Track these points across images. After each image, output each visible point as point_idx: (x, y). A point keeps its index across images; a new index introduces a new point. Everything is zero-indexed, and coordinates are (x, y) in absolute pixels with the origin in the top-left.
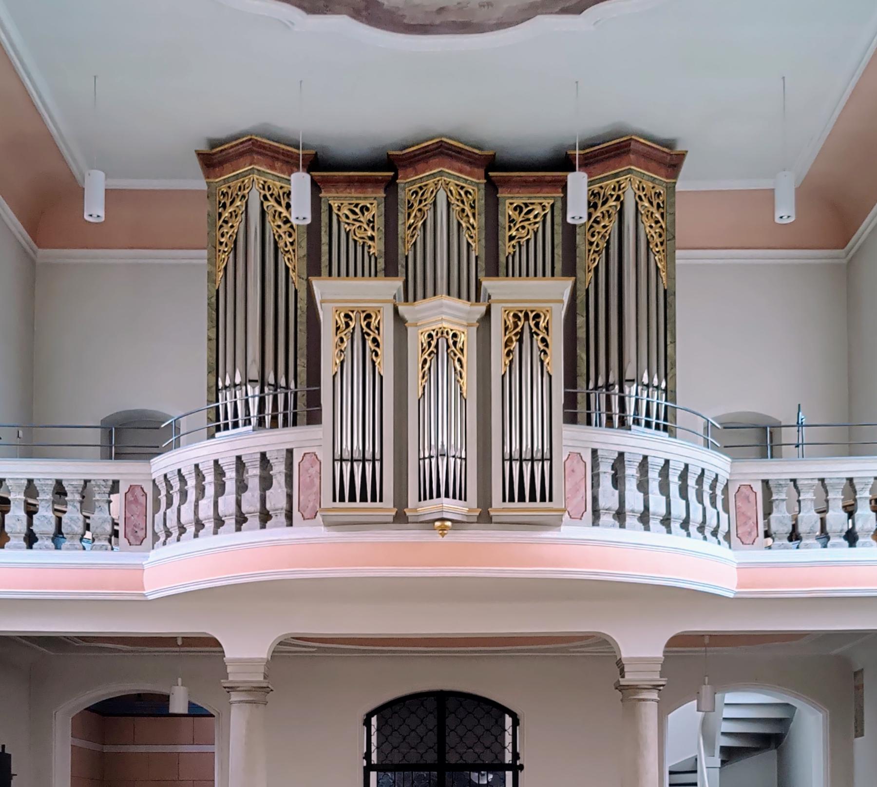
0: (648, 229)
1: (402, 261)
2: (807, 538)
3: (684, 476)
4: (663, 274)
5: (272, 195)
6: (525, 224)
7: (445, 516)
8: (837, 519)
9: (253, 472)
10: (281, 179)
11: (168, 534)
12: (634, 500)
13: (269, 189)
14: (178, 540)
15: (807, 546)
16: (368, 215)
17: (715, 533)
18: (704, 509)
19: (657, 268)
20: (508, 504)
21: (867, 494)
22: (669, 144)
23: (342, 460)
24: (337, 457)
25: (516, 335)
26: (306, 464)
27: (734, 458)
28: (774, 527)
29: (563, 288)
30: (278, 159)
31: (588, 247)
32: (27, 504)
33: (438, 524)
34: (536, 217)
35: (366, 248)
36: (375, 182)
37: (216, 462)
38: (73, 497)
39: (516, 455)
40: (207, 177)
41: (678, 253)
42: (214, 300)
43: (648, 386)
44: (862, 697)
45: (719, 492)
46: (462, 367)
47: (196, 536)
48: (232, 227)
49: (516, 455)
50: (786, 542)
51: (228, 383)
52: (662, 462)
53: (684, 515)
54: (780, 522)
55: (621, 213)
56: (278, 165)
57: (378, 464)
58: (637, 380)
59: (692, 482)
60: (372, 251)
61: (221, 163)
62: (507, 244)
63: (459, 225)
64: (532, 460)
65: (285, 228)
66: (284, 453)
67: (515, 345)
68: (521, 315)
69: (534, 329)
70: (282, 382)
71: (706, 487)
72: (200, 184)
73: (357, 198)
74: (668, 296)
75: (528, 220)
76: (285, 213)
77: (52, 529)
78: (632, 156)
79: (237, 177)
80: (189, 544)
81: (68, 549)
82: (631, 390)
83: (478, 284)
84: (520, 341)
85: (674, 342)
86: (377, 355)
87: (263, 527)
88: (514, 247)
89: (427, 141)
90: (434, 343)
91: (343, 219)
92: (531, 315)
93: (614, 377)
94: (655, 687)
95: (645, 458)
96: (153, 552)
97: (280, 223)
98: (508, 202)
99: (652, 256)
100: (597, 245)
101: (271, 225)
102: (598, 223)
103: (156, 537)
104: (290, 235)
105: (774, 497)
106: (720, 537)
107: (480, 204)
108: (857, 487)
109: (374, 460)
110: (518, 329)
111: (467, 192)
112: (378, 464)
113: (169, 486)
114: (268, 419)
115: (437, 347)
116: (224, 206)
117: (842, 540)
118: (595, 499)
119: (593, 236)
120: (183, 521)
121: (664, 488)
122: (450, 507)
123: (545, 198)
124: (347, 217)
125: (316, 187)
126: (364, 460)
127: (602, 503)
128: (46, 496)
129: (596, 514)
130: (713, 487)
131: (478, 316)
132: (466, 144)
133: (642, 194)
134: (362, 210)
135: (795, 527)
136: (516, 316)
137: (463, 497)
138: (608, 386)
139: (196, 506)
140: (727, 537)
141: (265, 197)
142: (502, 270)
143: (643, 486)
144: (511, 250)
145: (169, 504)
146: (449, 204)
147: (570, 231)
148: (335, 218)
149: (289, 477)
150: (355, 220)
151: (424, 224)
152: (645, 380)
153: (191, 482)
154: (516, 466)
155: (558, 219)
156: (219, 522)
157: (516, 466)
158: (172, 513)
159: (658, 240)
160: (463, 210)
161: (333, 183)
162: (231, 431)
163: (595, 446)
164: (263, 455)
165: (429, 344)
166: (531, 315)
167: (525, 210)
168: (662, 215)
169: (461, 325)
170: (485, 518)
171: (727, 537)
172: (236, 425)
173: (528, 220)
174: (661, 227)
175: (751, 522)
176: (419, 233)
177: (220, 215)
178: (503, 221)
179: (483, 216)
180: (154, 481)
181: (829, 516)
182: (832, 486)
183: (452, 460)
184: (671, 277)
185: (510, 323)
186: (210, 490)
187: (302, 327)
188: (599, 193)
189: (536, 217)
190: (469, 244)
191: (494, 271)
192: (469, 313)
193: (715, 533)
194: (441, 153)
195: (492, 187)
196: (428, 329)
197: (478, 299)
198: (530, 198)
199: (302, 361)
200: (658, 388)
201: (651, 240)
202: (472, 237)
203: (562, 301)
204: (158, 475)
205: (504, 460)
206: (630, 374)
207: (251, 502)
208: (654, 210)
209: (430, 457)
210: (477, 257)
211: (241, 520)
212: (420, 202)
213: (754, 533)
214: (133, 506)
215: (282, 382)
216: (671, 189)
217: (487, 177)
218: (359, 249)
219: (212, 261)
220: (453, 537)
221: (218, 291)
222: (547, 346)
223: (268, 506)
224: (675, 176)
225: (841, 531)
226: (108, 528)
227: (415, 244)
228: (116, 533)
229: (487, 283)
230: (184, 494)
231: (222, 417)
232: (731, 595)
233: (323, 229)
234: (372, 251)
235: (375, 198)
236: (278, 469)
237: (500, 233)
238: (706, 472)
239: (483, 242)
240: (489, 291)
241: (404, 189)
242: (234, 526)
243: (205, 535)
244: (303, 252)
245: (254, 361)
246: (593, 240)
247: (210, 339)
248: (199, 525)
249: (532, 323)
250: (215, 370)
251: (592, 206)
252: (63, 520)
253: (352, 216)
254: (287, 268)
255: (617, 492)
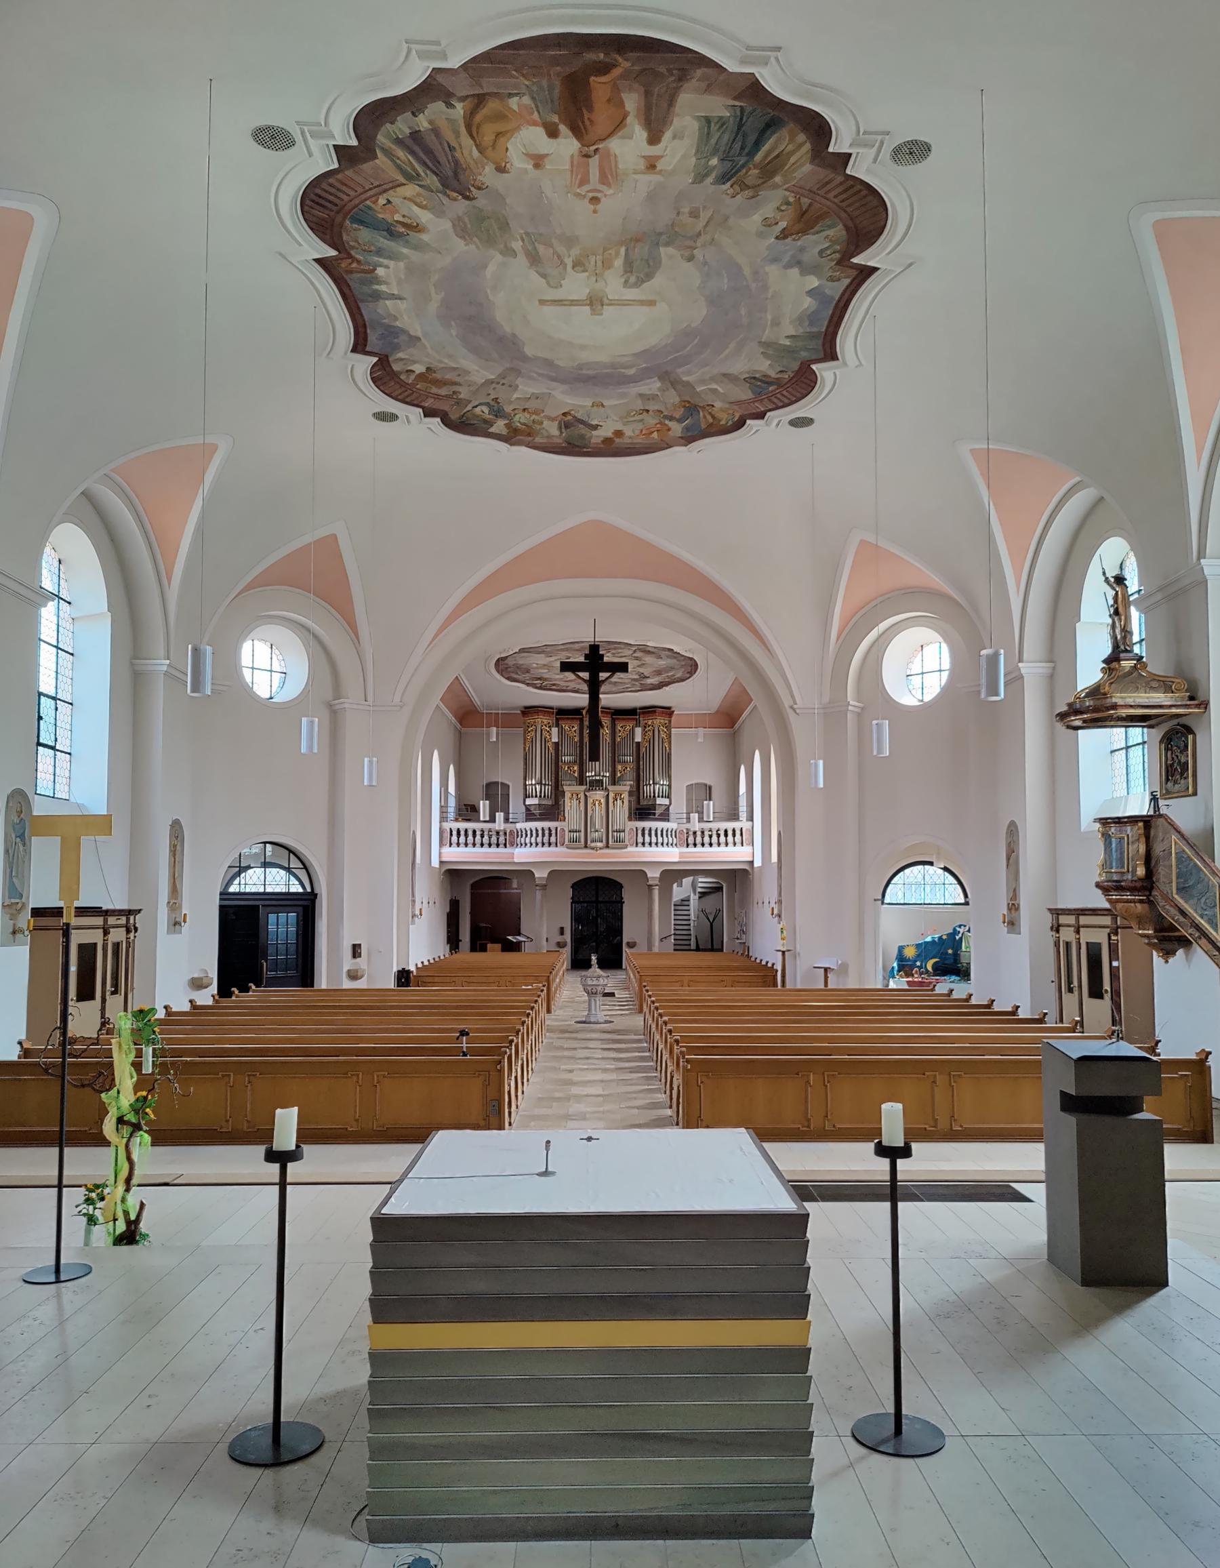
9: (547, 832)
93: (651, 782)
122: (599, 844)
129: (637, 844)
137: (602, 842)
156: (537, 844)
158: (523, 839)
170: (607, 846)
171: (676, 845)
236: (553, 832)
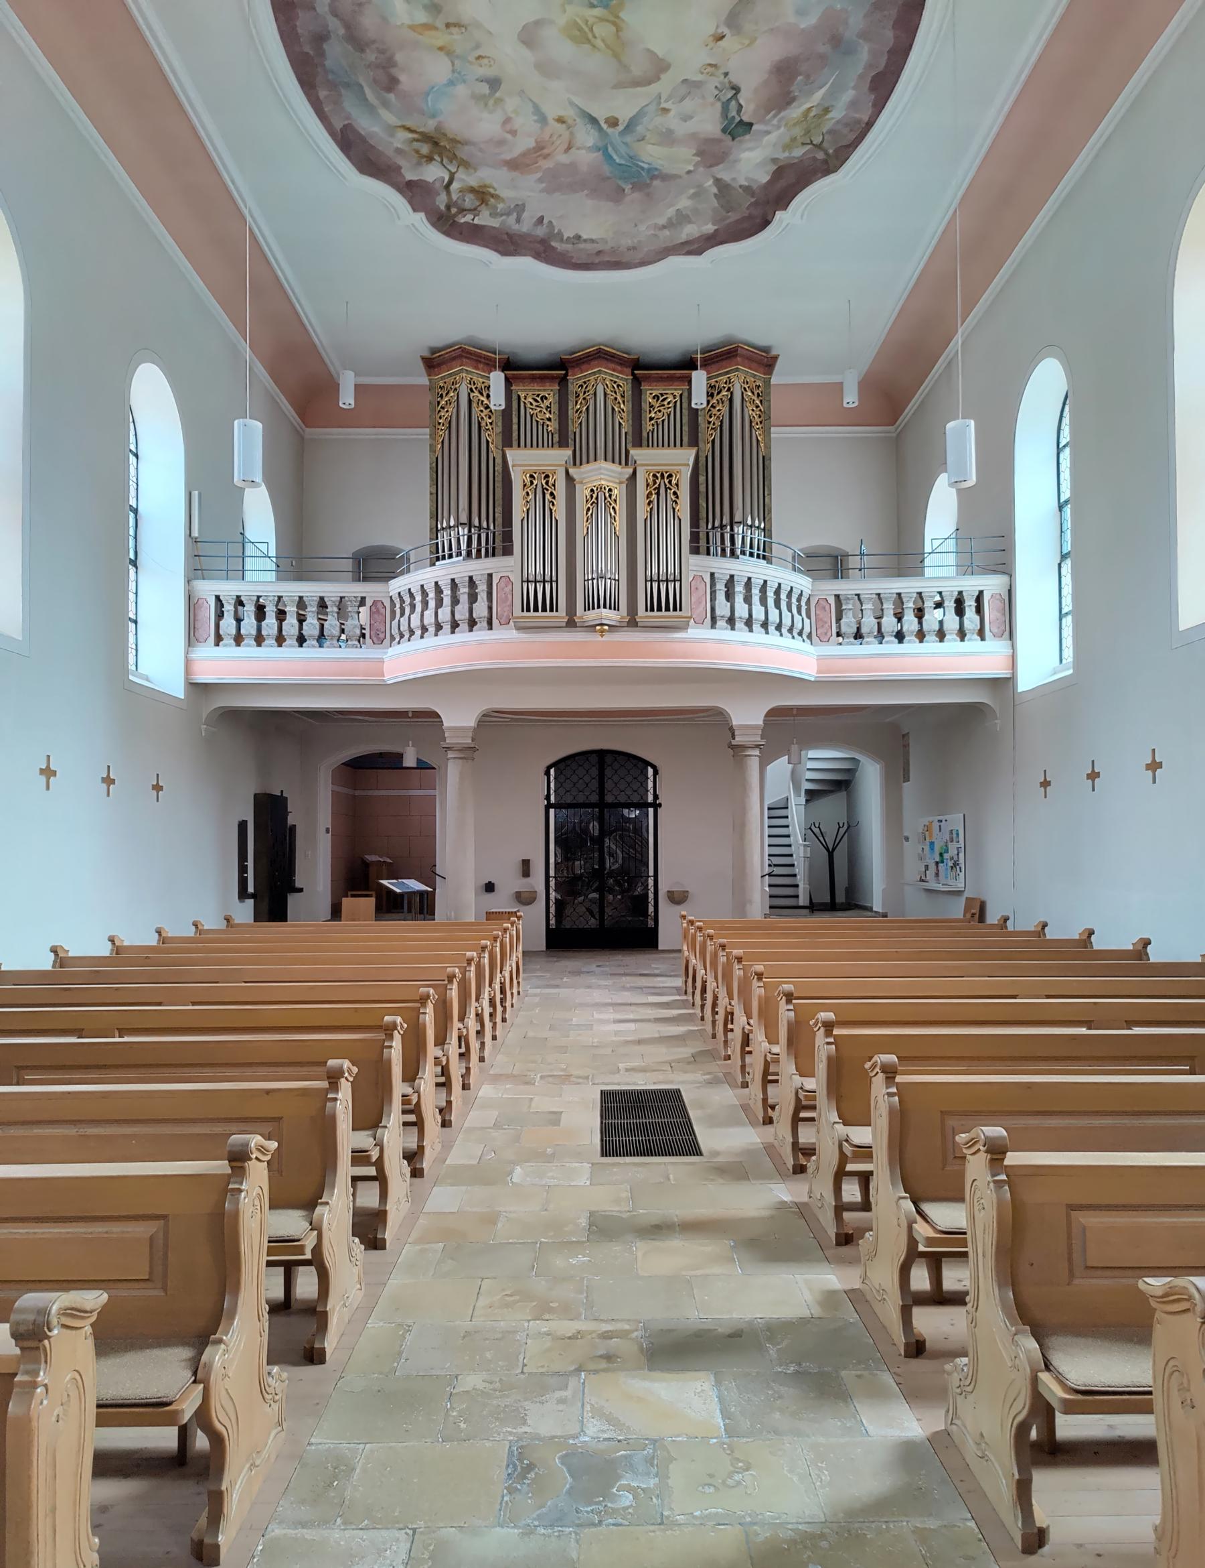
0: (751, 412)
1: (571, 436)
2: (868, 637)
3: (777, 592)
4: (762, 445)
5: (476, 388)
6: (661, 408)
7: (604, 622)
8: (889, 622)
9: (464, 590)
10: (482, 377)
11: (402, 636)
12: (741, 610)
13: (474, 384)
14: (409, 640)
15: (868, 643)
16: (547, 403)
17: (800, 634)
18: (793, 616)
19: (758, 440)
20: (649, 613)
21: (911, 605)
22: (766, 350)
23: (528, 581)
24: (525, 579)
25: (654, 489)
26: (502, 584)
27: (814, 579)
28: (843, 629)
29: (689, 455)
30: (480, 362)
31: (707, 425)
32: (298, 614)
33: (598, 628)
34: (669, 403)
35: (545, 427)
36: (552, 378)
37: (436, 583)
38: (332, 609)
39: (655, 578)
40: (429, 375)
41: (772, 429)
42: (434, 465)
43: (751, 526)
44: (908, 752)
45: (803, 603)
46: (615, 513)
47: (422, 637)
48: (447, 411)
49: (655, 578)
50: (853, 640)
51: (445, 525)
52: (762, 582)
53: (778, 621)
54: (848, 625)
55: (731, 400)
56: (481, 366)
57: (554, 584)
58: (743, 522)
59: (783, 596)
60: (550, 429)
61: (439, 365)
62: (648, 423)
63: (613, 409)
64: (667, 581)
65: (486, 412)
66: (486, 576)
67: (654, 497)
68: (659, 475)
69: (668, 485)
70: (485, 525)
71: (794, 600)
72: (424, 380)
73: (539, 390)
74: (765, 461)
75: (664, 405)
76: (486, 401)
77: (317, 632)
78: (739, 359)
79: (451, 375)
80: (417, 643)
81: (328, 647)
82: (739, 529)
83: (627, 452)
84: (658, 494)
85: (770, 494)
86: (553, 504)
87: (471, 630)
88: (653, 425)
89: (589, 348)
90: (595, 496)
91: (529, 405)
92: (666, 475)
93: (726, 520)
94: (758, 746)
95: (749, 579)
96: (390, 649)
97: (482, 409)
98: (648, 392)
99: (754, 431)
100: (714, 424)
101: (475, 410)
102: (714, 407)
103: (392, 638)
104: (490, 418)
105: (844, 607)
106: (804, 636)
107: (628, 394)
108: (904, 600)
109: (551, 581)
110: (657, 485)
111: (618, 386)
112: (554, 584)
113: (402, 601)
114: (474, 552)
115: (597, 498)
116: (441, 396)
117: (893, 639)
118: (713, 609)
119: (711, 417)
120: (412, 626)
121: (763, 601)
122: (607, 615)
123: (675, 389)
124: (531, 404)
125: (508, 382)
126: (544, 582)
127: (718, 612)
128: (312, 609)
129: (714, 620)
130: (799, 600)
131: (627, 476)
132: (618, 351)
133: (746, 386)
134: (542, 399)
135: (859, 629)
136: (654, 476)
138: (722, 527)
139: (422, 616)
140: (810, 636)
141: (471, 390)
142: (644, 442)
143: (748, 600)
144: (651, 428)
145: (402, 614)
146: (605, 394)
147: (694, 413)
148: (522, 404)
149: (490, 594)
150: (537, 406)
151: (587, 409)
152: (749, 522)
153: (418, 598)
154: (655, 585)
155: (685, 405)
156: (439, 627)
157: (655, 585)
158: (404, 621)
159: (758, 420)
160: (616, 399)
161: (521, 379)
162: (448, 561)
163: (713, 571)
164: (471, 578)
165: (592, 497)
166: (666, 475)
167: (661, 399)
168: (761, 401)
169: (615, 482)
170: (633, 623)
171: (810, 636)
172: (450, 556)
173: (664, 405)
174: (760, 410)
175: (827, 626)
176: (584, 415)
177: (439, 403)
178: (645, 407)
179: (630, 403)
180: (391, 597)
181: (884, 621)
182: (886, 598)
183: (608, 581)
184: (768, 447)
185: (651, 480)
186: (432, 604)
187: (499, 485)
188: (715, 386)
189: (669, 403)
190: (620, 424)
191: (638, 443)
192: (620, 473)
193: (800, 634)
194: (600, 357)
195: (637, 382)
196: (590, 485)
197: (627, 464)
198: (664, 390)
199: (499, 509)
200: (758, 528)
201: (753, 420)
202: (622, 418)
203: (688, 465)
204: (394, 593)
205: (646, 581)
206: (738, 517)
207: (462, 612)
208: (755, 398)
209: (593, 579)
210: (626, 433)
211: (455, 625)
212: (585, 393)
213: (829, 634)
214: (376, 616)
215: (485, 525)
216: (767, 383)
217: (633, 374)
218: (540, 427)
219: (433, 436)
220: (608, 637)
221: (437, 458)
222: (677, 497)
223: (474, 616)
224: (770, 373)
225: (893, 632)
226: (358, 632)
227: (581, 423)
228: (363, 636)
229: (632, 452)
230: (413, 607)
231: (440, 551)
232: (813, 679)
233: (514, 413)
234: (550, 429)
235: (552, 390)
236: (482, 588)
237: (643, 415)
238: (794, 589)
239: (630, 422)
240: (635, 458)
241: (573, 383)
242: (449, 630)
243: (429, 637)
244: (499, 429)
245: (464, 509)
246: (711, 420)
247: (431, 494)
248: (424, 629)
249: (666, 481)
250: (435, 516)
251: (710, 395)
252: (326, 626)
253: (534, 403)
254: (488, 442)
255: (729, 604)
